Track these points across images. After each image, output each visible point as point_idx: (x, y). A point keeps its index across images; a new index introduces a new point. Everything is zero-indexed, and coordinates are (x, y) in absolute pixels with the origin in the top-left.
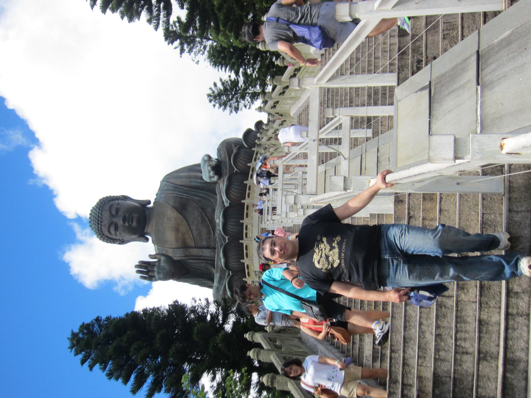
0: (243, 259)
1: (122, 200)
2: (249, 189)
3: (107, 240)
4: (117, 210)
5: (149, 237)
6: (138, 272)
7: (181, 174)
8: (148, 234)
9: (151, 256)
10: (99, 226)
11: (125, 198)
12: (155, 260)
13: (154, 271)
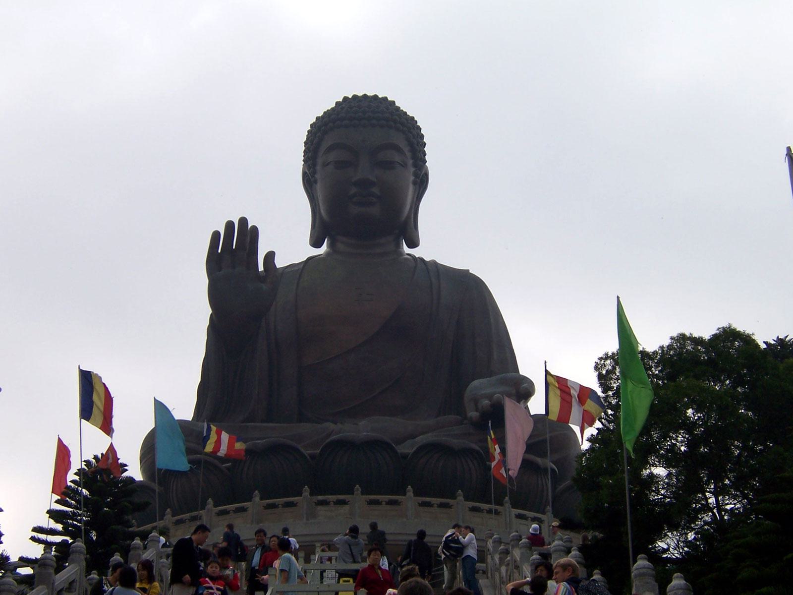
0: (262, 499)
1: (416, 175)
2: (442, 505)
4: (389, 165)
5: (323, 249)
6: (230, 225)
8: (331, 245)
9: (270, 256)
10: (346, 122)
11: (422, 182)
12: (261, 268)
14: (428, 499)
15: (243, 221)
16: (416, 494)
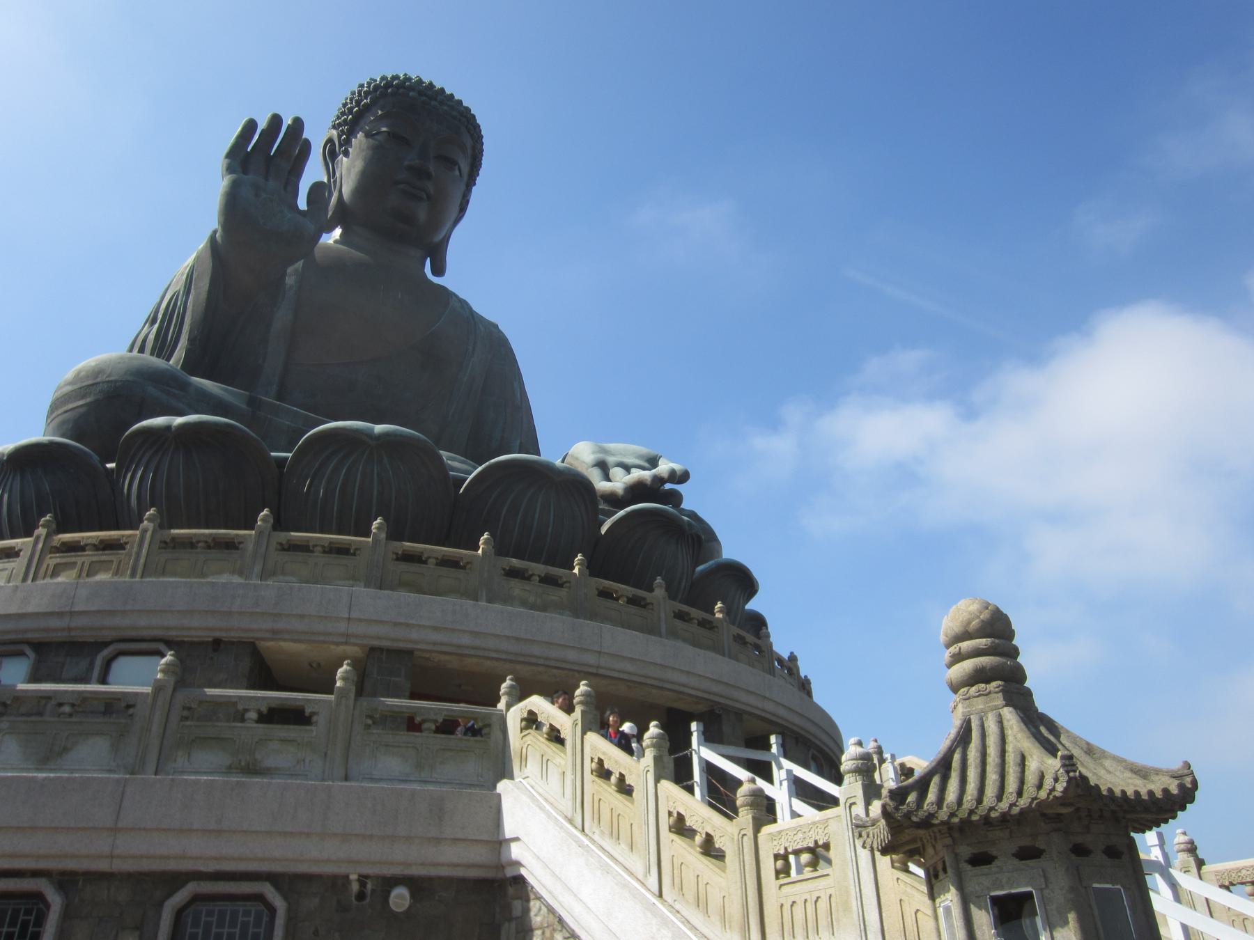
6: (276, 120)
11: (463, 209)
13: (266, 179)
14: (685, 608)
15: (298, 124)
16: (672, 594)
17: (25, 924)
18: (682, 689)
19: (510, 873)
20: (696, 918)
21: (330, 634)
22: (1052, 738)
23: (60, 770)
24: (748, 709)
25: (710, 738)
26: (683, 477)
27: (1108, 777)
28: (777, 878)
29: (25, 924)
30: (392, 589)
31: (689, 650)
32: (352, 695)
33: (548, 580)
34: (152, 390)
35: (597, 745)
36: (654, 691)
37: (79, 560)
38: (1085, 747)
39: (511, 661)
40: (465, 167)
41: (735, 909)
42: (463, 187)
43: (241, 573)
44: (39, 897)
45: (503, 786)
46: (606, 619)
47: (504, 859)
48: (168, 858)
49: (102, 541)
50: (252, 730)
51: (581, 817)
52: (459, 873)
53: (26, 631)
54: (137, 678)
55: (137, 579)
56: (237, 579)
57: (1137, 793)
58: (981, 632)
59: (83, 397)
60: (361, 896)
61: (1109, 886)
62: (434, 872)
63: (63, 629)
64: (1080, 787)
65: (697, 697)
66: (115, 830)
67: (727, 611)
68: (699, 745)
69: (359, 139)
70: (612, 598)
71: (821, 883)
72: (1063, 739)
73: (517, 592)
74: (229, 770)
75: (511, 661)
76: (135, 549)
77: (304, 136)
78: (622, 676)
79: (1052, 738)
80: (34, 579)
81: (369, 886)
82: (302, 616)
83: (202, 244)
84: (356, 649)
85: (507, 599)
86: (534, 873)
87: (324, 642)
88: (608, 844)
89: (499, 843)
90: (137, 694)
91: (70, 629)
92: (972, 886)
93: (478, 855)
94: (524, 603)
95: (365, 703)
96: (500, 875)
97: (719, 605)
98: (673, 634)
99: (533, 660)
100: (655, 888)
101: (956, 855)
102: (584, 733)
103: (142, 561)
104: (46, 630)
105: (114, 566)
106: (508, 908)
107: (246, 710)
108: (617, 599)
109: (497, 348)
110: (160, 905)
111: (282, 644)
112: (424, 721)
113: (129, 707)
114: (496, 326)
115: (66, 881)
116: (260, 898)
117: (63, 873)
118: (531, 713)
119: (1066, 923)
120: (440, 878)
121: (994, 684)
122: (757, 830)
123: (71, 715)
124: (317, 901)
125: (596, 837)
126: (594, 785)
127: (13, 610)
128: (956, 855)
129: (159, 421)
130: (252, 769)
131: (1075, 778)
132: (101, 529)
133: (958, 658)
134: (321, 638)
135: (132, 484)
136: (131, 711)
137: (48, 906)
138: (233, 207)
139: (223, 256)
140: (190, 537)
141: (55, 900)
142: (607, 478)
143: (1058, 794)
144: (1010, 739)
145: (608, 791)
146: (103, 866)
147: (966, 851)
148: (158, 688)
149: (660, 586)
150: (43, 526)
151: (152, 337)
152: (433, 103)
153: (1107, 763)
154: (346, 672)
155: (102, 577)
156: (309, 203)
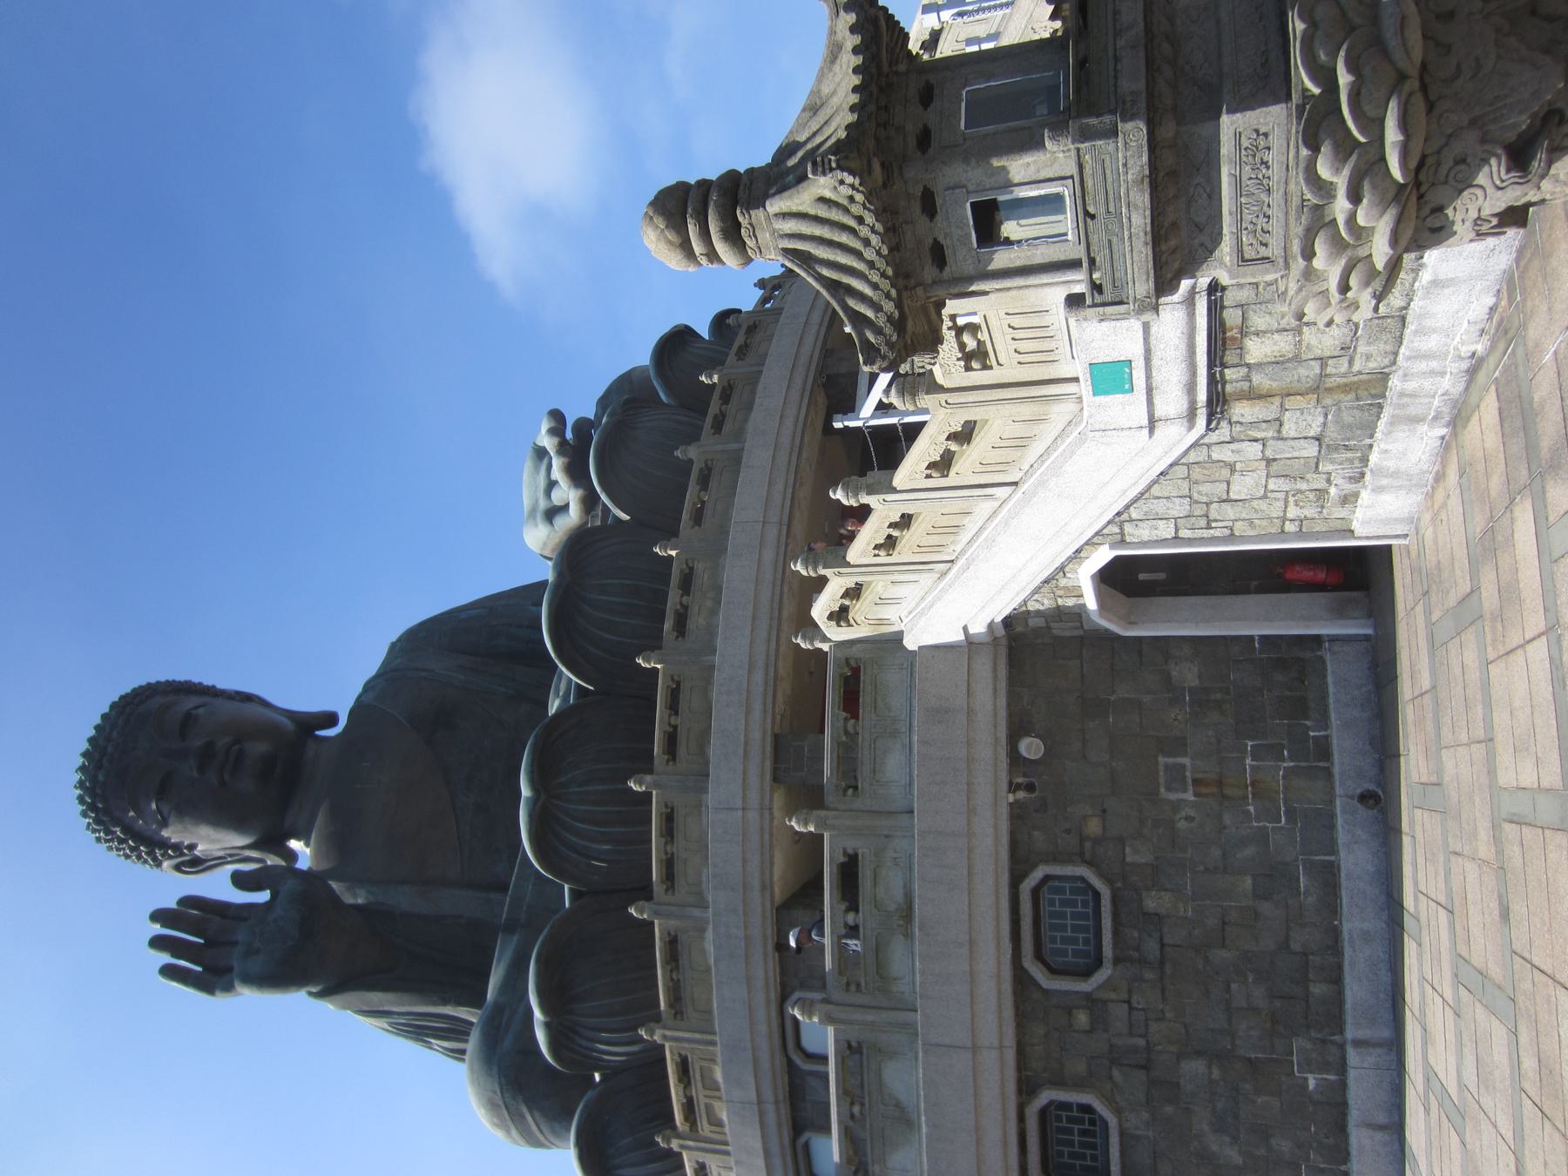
3: (121, 841)
6: (157, 943)
7: (463, 616)
11: (248, 698)
13: (236, 943)
14: (709, 420)
15: (159, 916)
16: (693, 437)
17: (1070, 1120)
18: (800, 424)
19: (1001, 632)
20: (1037, 448)
21: (762, 829)
22: (800, 154)
23: (918, 1107)
24: (819, 343)
25: (850, 407)
26: (557, 416)
27: (841, 93)
28: (991, 368)
29: (1070, 1120)
30: (707, 762)
31: (756, 416)
32: (823, 813)
33: (686, 584)
34: (507, 1043)
35: (858, 551)
36: (804, 455)
37: (703, 1101)
38: (808, 114)
39: (779, 624)
40: (190, 702)
41: (1026, 410)
42: (219, 701)
43: (703, 930)
44: (1043, 1112)
45: (911, 643)
46: (726, 515)
47: (988, 639)
48: (999, 992)
49: (680, 1080)
50: (866, 916)
51: (936, 564)
52: (1003, 685)
53: (782, 1146)
54: (821, 1035)
55: (717, 1038)
56: (709, 934)
57: (856, 70)
58: (681, 229)
59: (522, 1116)
60: (1030, 788)
61: (963, 105)
62: (1003, 713)
63: (778, 1109)
64: (847, 153)
65: (809, 405)
66: (975, 1049)
67: (710, 367)
68: (858, 419)
69: (171, 834)
70: (702, 508)
71: (993, 323)
72: (802, 138)
73: (701, 621)
74: (908, 935)
75: (779, 624)
76: (686, 1045)
77: (173, 905)
78: (789, 496)
79: (800, 154)
80: (726, 1143)
81: (1020, 780)
82: (745, 861)
83: (327, 1007)
84: (776, 796)
85: (711, 632)
86: (1000, 609)
87: (771, 834)
88: (965, 537)
89: (971, 643)
90: (836, 1041)
91: (777, 1102)
92: (969, 268)
93: (983, 667)
94: (714, 612)
95: (830, 798)
96: (1004, 642)
97: (703, 378)
98: (739, 435)
99: (777, 598)
100: (1009, 489)
101: (934, 282)
102: (848, 565)
103: (697, 1036)
104: (779, 1125)
105: (705, 1064)
106: (1037, 631)
107: (846, 925)
108: (703, 503)
109: (422, 642)
110: (1046, 992)
111: (776, 878)
112: (846, 732)
113: (850, 1046)
114: (393, 645)
115: (1026, 1088)
116: (1036, 892)
117: (1020, 1091)
118: (831, 617)
119: (1004, 168)
120: (1009, 705)
121: (740, 219)
122: (941, 389)
123: (863, 1105)
124: (1036, 833)
125: (958, 548)
126: (903, 553)
127: (761, 1162)
128: (934, 282)
129: (541, 1036)
130: (907, 912)
131: (837, 161)
132: (666, 1077)
133: (713, 256)
134: (767, 836)
135: (614, 1052)
136: (854, 1044)
137: (1051, 1103)
138: (279, 976)
139: (336, 981)
140: (667, 990)
141: (1046, 1096)
142: (565, 508)
143: (857, 182)
144: (802, 209)
145: (909, 541)
146: (1010, 1055)
147: (929, 273)
148: (829, 1019)
149: (684, 452)
150: (669, 1142)
151: (446, 1044)
152: (110, 749)
153: (826, 90)
154: (798, 823)
155: (719, 1075)
156: (258, 888)
